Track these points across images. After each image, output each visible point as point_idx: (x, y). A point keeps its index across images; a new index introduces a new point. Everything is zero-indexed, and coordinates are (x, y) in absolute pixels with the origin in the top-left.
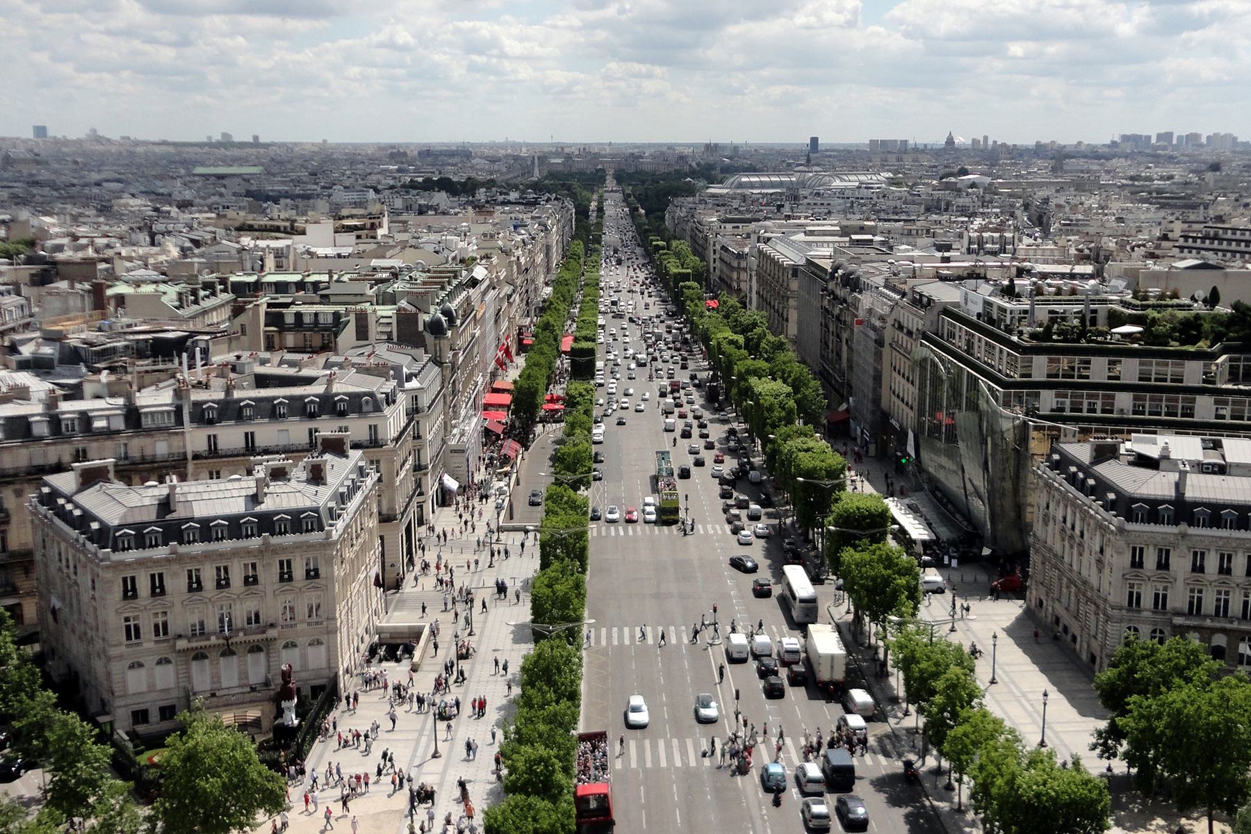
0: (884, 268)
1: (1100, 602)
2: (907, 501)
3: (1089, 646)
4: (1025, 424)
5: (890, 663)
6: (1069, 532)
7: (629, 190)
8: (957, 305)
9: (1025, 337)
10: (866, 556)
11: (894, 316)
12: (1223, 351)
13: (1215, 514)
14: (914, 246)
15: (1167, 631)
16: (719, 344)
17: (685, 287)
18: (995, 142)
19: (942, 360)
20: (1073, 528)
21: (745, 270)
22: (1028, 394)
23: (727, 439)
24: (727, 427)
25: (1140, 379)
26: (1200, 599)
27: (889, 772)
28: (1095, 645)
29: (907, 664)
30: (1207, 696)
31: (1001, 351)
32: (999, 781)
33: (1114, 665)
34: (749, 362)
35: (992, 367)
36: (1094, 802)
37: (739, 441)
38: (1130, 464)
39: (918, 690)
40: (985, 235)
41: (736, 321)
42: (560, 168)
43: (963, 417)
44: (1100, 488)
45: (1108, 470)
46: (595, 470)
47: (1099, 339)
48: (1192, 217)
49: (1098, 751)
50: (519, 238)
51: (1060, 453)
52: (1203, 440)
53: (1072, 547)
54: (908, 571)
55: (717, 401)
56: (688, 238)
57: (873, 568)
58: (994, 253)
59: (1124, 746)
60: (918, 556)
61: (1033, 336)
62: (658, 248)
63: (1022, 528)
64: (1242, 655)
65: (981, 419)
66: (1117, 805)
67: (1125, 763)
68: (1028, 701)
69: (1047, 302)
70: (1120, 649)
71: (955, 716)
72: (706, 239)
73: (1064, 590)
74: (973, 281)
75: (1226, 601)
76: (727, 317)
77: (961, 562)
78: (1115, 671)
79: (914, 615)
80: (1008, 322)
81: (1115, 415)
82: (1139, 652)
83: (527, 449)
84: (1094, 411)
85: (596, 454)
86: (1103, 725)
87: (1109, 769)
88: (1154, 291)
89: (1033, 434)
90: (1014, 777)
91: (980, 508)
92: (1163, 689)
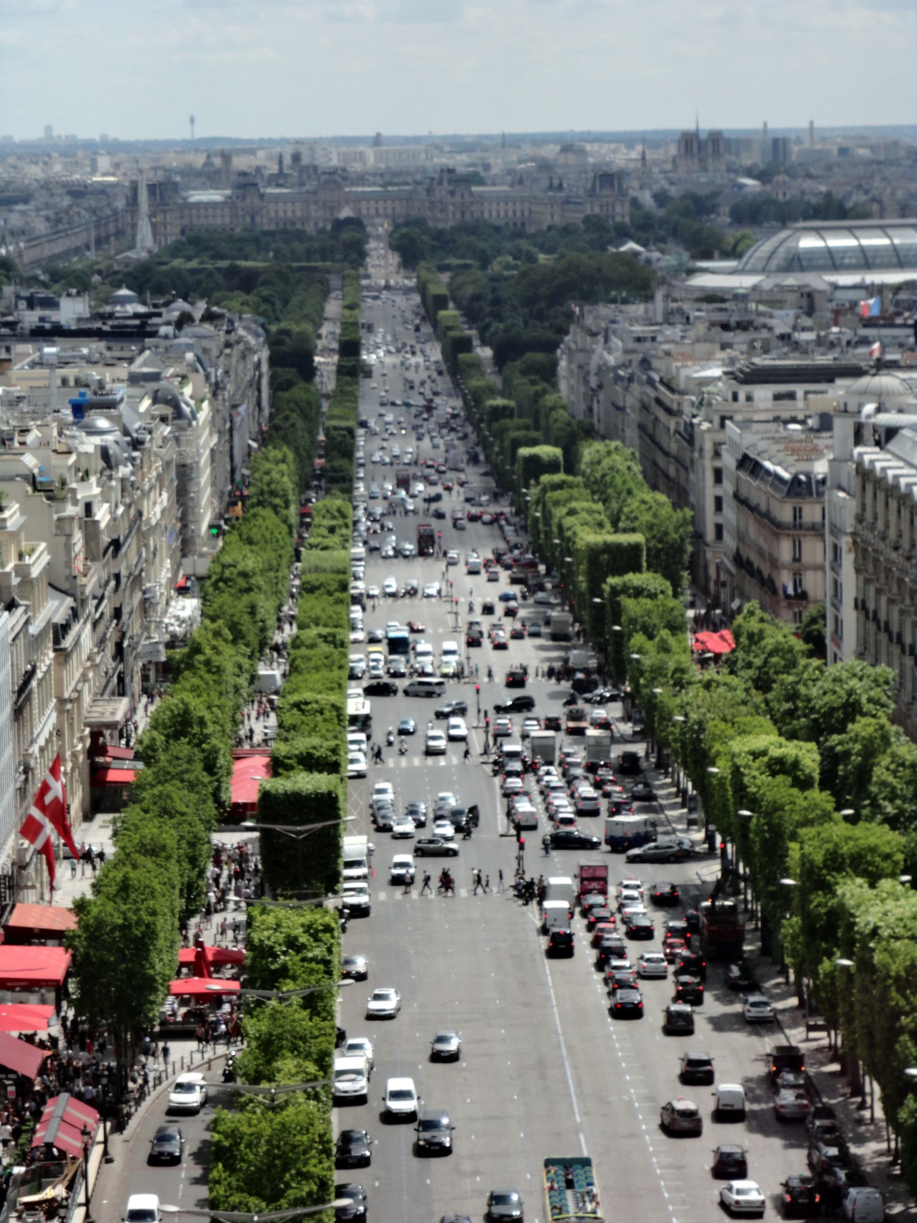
7: (441, 283)
16: (736, 772)
17: (624, 589)
21: (817, 530)
23: (772, 1083)
24: (768, 1043)
34: (838, 830)
37: (810, 1089)
41: (793, 696)
42: (221, 220)
46: (341, 1191)
50: (90, 444)
55: (736, 955)
56: (632, 433)
62: (536, 466)
72: (689, 435)
76: (763, 684)
83: (119, 1127)
85: (347, 1138)
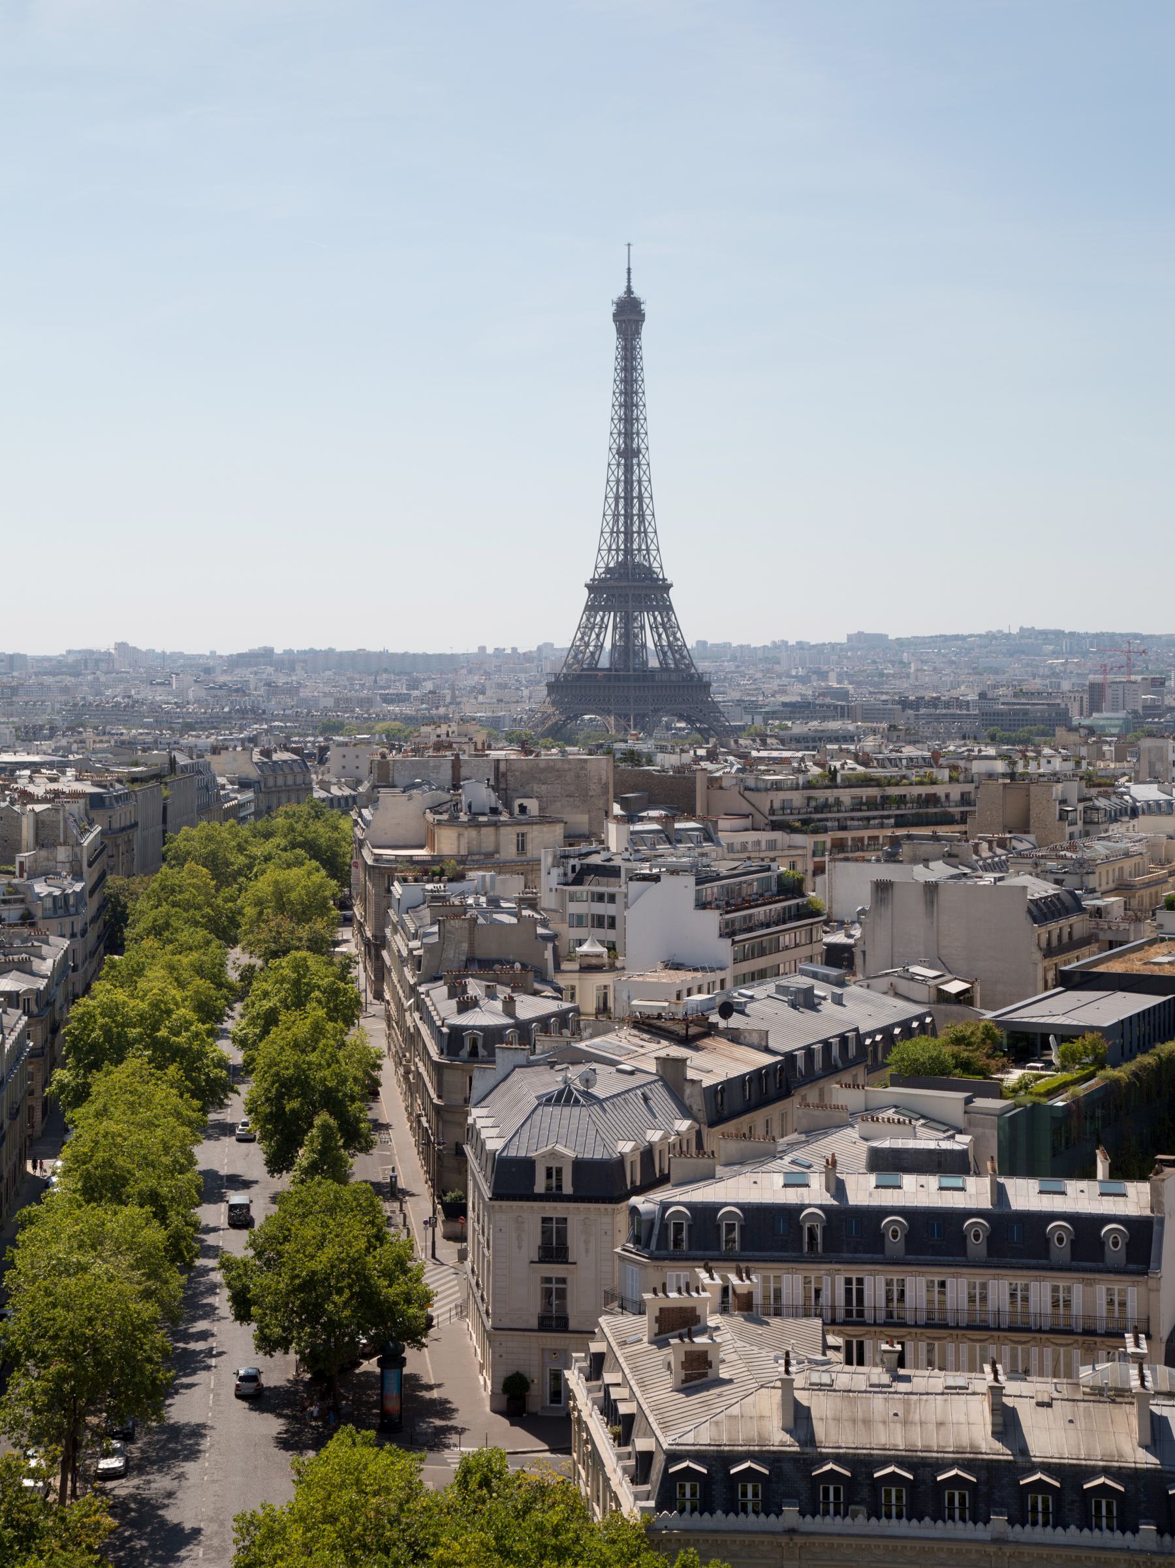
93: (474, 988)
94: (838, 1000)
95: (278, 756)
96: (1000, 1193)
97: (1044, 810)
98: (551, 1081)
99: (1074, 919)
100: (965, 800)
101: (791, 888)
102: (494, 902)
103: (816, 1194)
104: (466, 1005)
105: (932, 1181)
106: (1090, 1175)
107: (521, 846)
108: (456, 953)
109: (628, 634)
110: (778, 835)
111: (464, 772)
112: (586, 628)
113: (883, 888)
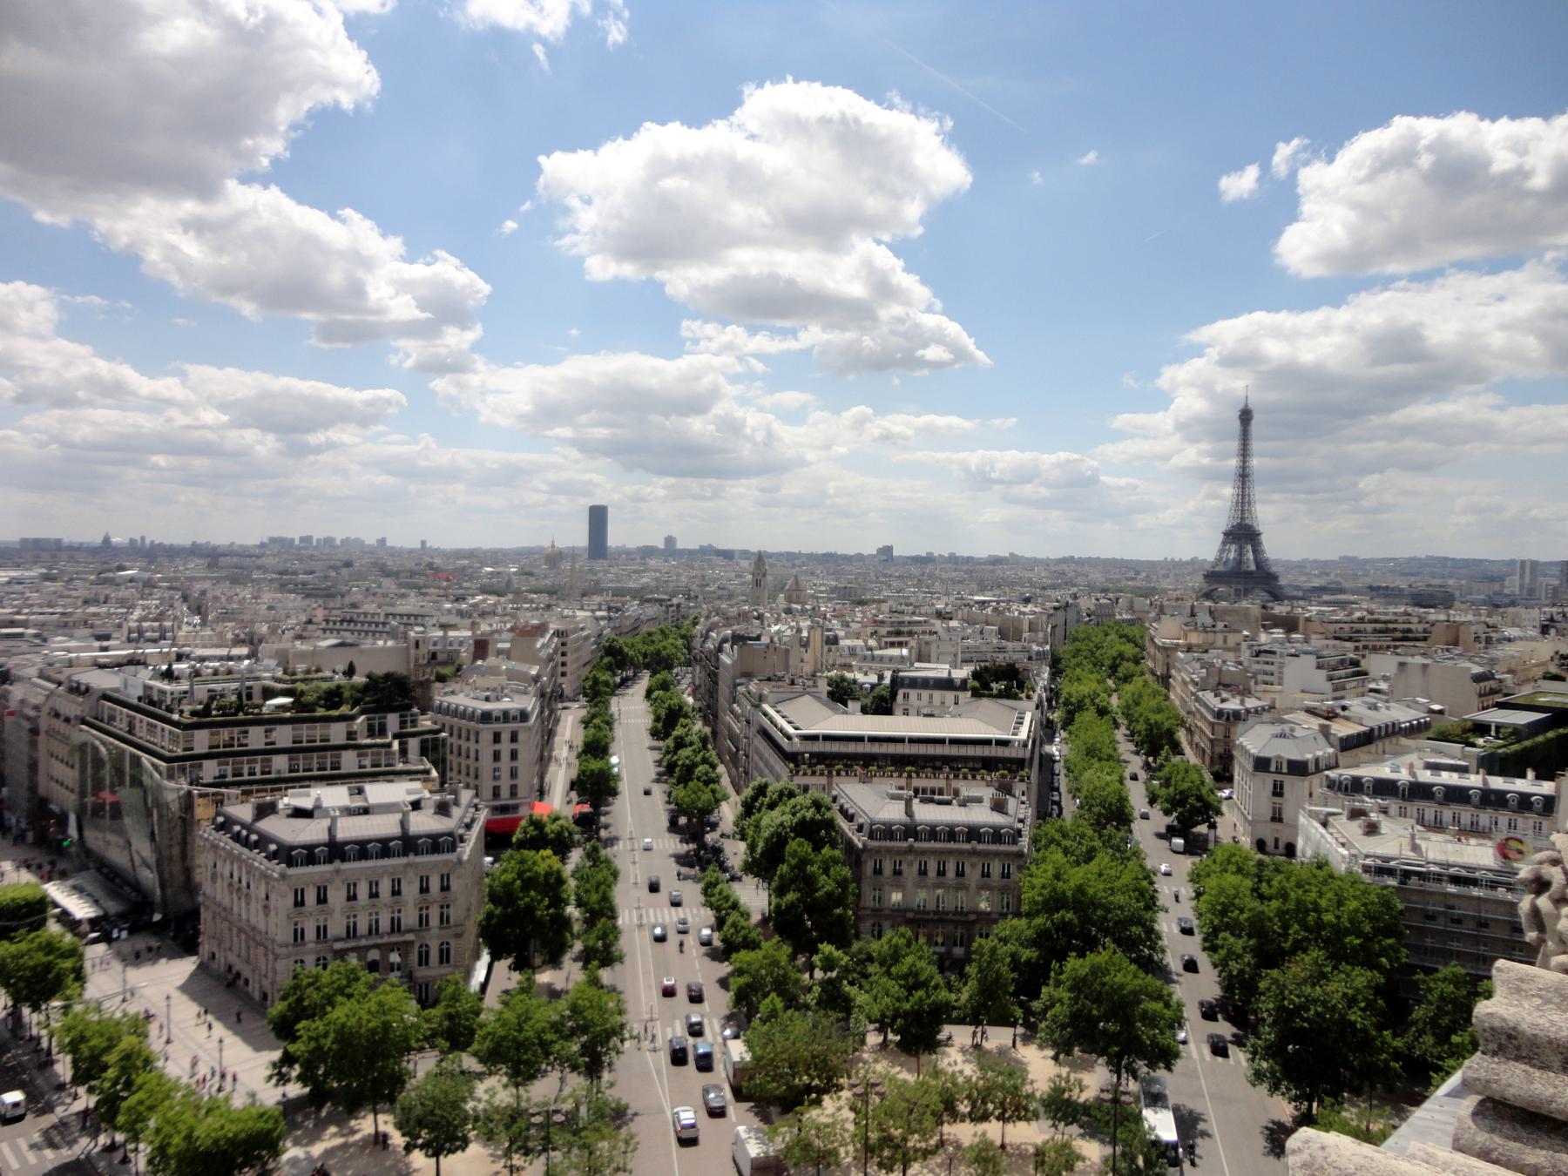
0: (38, 659)
1: (268, 944)
2: (71, 882)
3: (261, 986)
4: (189, 793)
5: (55, 1050)
6: (236, 886)
8: (116, 690)
9: (186, 714)
10: (23, 946)
11: (50, 704)
12: (362, 712)
13: (363, 849)
14: (71, 637)
15: (329, 956)
18: (152, 542)
19: (104, 743)
20: (240, 881)
22: (191, 766)
25: (294, 742)
26: (355, 924)
27: (56, 1164)
28: (266, 983)
29: (73, 1047)
30: (366, 1006)
31: (163, 730)
32: (176, 1140)
33: (284, 998)
35: (155, 744)
36: (270, 1132)
38: (289, 816)
39: (88, 1070)
40: (145, 624)
43: (127, 795)
44: (262, 842)
45: (268, 825)
47: (256, 711)
48: (331, 605)
49: (274, 1081)
51: (224, 815)
52: (350, 789)
53: (240, 898)
54: (74, 953)
57: (31, 958)
58: (155, 641)
59: (296, 1070)
60: (82, 936)
61: (194, 713)
63: (191, 887)
64: (392, 964)
65: (145, 792)
66: (294, 1126)
67: (299, 1085)
68: (205, 1051)
69: (205, 682)
70: (289, 982)
71: (128, 1085)
73: (235, 939)
74: (132, 668)
75: (377, 921)
77: (132, 932)
78: (286, 1003)
79: (80, 995)
80: (169, 702)
81: (273, 776)
82: (304, 983)
84: (254, 774)
86: (277, 1055)
87: (284, 1095)
88: (300, 667)
89: (198, 801)
90: (191, 1129)
91: (148, 877)
92: (329, 1009)
93: (1225, 695)
94: (1388, 708)
95: (1102, 601)
96: (1485, 782)
97: (1467, 635)
98: (1277, 729)
99: (1491, 682)
100: (1425, 631)
101: (1355, 663)
102: (1224, 662)
103: (1403, 776)
104: (1223, 701)
105: (1455, 775)
106: (1524, 776)
107: (1225, 641)
108: (1214, 680)
109: (1241, 553)
110: (1337, 642)
111: (1196, 610)
112: (1222, 551)
113: (1402, 664)
